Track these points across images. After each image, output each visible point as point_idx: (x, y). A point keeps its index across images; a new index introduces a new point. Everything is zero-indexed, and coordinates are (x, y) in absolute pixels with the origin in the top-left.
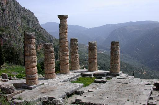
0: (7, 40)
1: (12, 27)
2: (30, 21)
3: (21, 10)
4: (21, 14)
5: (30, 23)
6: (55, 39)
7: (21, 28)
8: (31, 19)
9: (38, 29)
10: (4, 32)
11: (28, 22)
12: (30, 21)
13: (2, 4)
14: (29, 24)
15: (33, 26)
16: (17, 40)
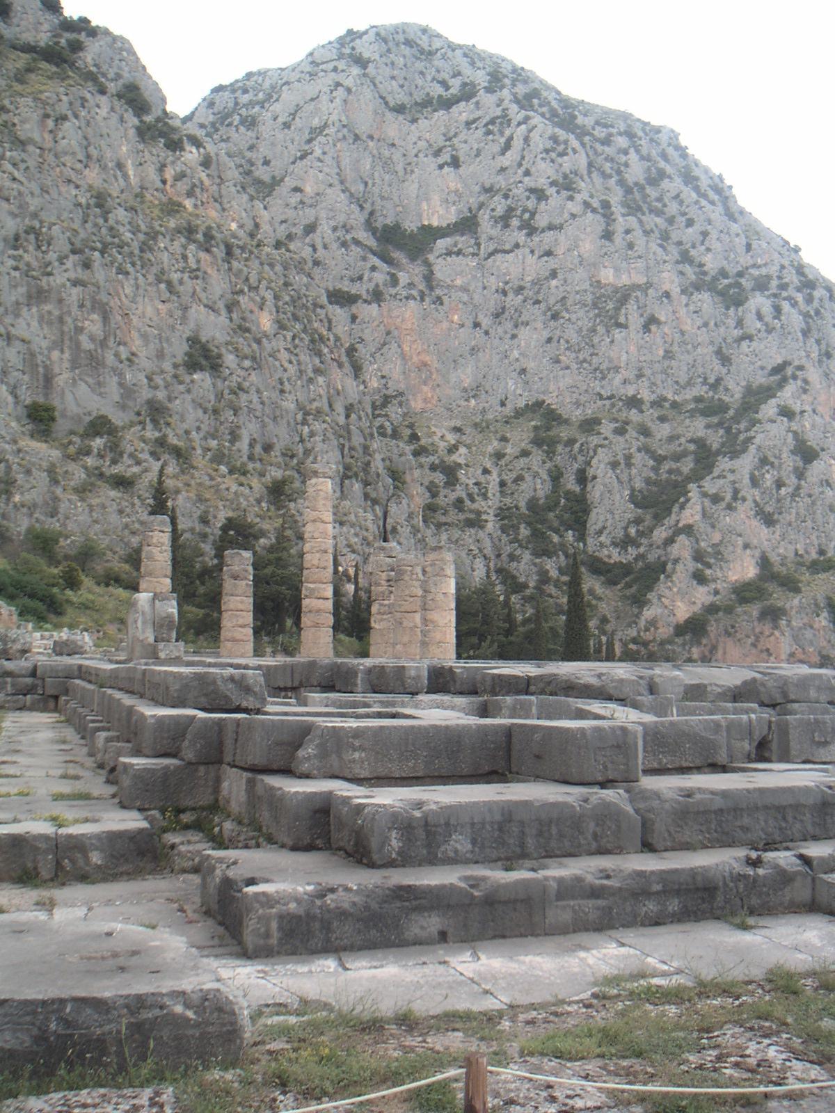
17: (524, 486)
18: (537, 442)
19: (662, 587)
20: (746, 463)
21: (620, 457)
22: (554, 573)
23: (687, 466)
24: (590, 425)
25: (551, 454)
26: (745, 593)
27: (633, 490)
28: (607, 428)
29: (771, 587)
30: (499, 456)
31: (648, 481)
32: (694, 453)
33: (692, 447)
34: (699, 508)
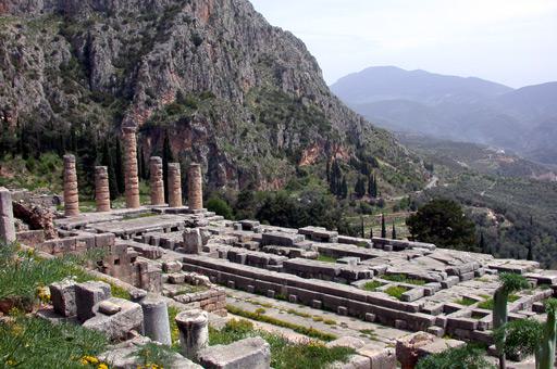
0: (204, 134)
1: (223, 92)
2: (284, 70)
3: (259, 35)
4: (256, 48)
5: (285, 79)
6: (372, 128)
7: (255, 96)
8: (291, 65)
9: (312, 97)
10: (195, 108)
11: (278, 75)
12: (284, 70)
13: (194, 21)
14: (280, 82)
15: (296, 88)
16: (234, 134)
17: (58, 56)
18: (60, 33)
19: (132, 107)
20: (169, 46)
21: (106, 42)
22: (76, 102)
23: (138, 46)
24: (89, 24)
25: (69, 40)
26: (170, 110)
27: (113, 60)
28: (98, 26)
29: (182, 107)
30: (42, 41)
31: (119, 55)
32: (142, 39)
33: (141, 36)
34: (147, 69)
